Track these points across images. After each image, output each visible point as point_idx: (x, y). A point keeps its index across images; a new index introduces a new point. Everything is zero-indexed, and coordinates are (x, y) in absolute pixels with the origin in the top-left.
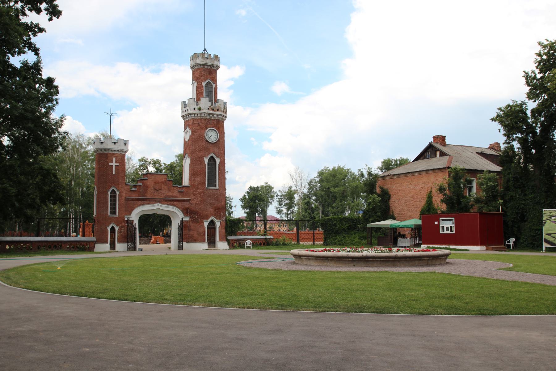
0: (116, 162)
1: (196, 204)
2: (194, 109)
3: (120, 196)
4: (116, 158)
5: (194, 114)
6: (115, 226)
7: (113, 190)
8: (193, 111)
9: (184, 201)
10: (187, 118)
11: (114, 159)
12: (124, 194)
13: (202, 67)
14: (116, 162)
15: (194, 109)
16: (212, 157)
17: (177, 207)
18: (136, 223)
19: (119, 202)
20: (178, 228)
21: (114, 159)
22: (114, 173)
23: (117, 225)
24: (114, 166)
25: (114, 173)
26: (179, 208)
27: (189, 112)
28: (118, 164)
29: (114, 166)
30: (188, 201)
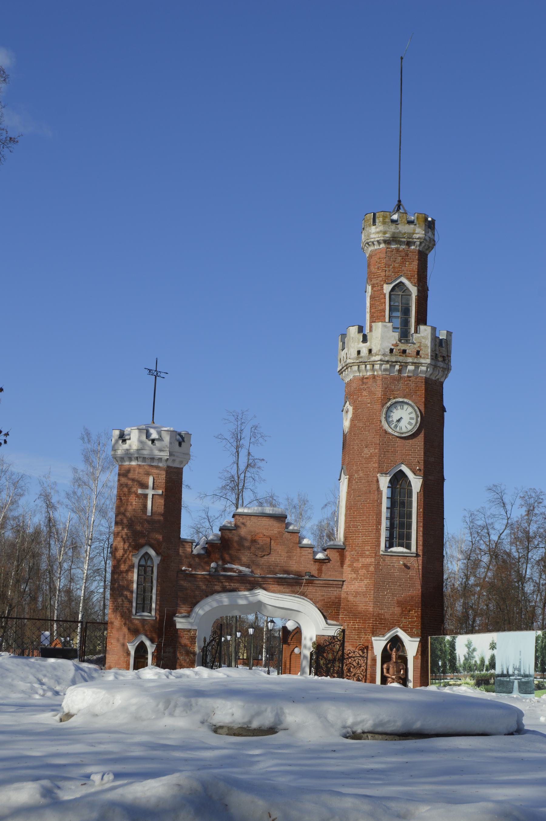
1: (357, 594)
6: (148, 643)
13: (382, 246)
23: (152, 641)
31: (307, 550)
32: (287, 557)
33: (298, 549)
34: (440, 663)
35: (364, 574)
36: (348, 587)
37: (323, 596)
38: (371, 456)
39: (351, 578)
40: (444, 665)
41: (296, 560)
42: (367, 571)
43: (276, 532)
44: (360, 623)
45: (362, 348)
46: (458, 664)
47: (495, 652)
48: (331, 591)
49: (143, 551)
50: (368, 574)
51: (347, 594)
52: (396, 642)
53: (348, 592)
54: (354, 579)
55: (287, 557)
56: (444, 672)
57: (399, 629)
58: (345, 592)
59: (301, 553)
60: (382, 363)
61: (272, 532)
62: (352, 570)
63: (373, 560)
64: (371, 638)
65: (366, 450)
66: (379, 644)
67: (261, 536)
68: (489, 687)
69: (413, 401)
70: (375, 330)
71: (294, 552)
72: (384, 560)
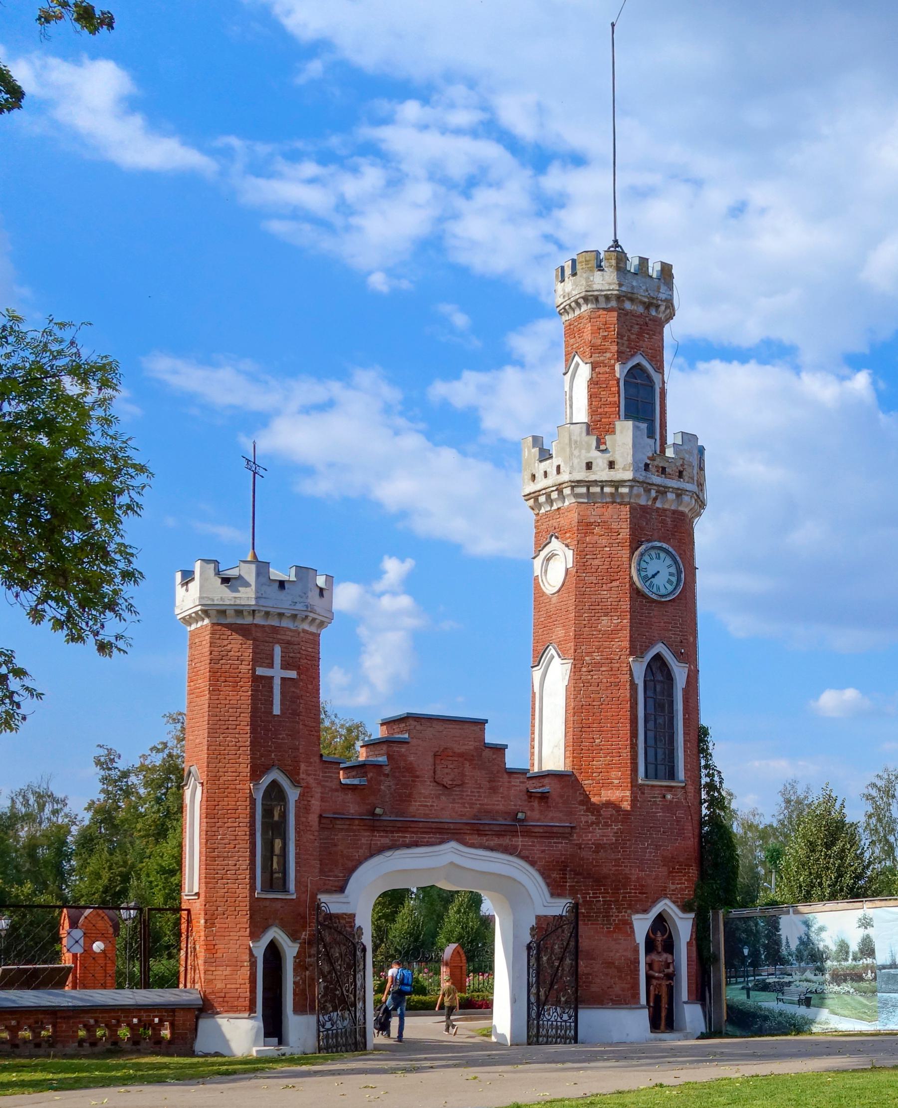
0: (285, 666)
1: (599, 847)
2: (589, 466)
3: (303, 807)
4: (287, 645)
5: (589, 484)
7: (274, 784)
8: (582, 475)
9: (550, 834)
10: (550, 501)
11: (278, 650)
12: (316, 804)
14: (285, 666)
15: (589, 466)
16: (658, 657)
17: (525, 858)
18: (365, 921)
19: (298, 832)
20: (529, 947)
21: (278, 650)
22: (277, 710)
24: (277, 684)
25: (277, 710)
26: (532, 864)
27: (565, 477)
28: (293, 674)
29: (277, 684)
30: (567, 834)
31: (518, 778)
32: (490, 789)
33: (506, 776)
34: (746, 952)
35: (612, 815)
36: (581, 836)
37: (543, 851)
38: (615, 631)
39: (587, 822)
40: (755, 954)
41: (502, 793)
42: (617, 811)
43: (472, 747)
44: (608, 893)
45: (596, 458)
46: (784, 951)
47: (870, 931)
48: (555, 843)
49: (266, 780)
50: (620, 815)
51: (580, 848)
52: (661, 922)
53: (580, 844)
54: (593, 823)
55: (490, 789)
56: (756, 964)
57: (667, 901)
58: (577, 845)
59: (509, 782)
60: (633, 484)
61: (466, 747)
62: (588, 810)
63: (628, 793)
64: (630, 916)
65: (605, 621)
66: (641, 925)
67: (451, 754)
68: (864, 985)
69: (672, 547)
70: (621, 432)
71: (499, 781)
72: (643, 793)
